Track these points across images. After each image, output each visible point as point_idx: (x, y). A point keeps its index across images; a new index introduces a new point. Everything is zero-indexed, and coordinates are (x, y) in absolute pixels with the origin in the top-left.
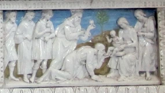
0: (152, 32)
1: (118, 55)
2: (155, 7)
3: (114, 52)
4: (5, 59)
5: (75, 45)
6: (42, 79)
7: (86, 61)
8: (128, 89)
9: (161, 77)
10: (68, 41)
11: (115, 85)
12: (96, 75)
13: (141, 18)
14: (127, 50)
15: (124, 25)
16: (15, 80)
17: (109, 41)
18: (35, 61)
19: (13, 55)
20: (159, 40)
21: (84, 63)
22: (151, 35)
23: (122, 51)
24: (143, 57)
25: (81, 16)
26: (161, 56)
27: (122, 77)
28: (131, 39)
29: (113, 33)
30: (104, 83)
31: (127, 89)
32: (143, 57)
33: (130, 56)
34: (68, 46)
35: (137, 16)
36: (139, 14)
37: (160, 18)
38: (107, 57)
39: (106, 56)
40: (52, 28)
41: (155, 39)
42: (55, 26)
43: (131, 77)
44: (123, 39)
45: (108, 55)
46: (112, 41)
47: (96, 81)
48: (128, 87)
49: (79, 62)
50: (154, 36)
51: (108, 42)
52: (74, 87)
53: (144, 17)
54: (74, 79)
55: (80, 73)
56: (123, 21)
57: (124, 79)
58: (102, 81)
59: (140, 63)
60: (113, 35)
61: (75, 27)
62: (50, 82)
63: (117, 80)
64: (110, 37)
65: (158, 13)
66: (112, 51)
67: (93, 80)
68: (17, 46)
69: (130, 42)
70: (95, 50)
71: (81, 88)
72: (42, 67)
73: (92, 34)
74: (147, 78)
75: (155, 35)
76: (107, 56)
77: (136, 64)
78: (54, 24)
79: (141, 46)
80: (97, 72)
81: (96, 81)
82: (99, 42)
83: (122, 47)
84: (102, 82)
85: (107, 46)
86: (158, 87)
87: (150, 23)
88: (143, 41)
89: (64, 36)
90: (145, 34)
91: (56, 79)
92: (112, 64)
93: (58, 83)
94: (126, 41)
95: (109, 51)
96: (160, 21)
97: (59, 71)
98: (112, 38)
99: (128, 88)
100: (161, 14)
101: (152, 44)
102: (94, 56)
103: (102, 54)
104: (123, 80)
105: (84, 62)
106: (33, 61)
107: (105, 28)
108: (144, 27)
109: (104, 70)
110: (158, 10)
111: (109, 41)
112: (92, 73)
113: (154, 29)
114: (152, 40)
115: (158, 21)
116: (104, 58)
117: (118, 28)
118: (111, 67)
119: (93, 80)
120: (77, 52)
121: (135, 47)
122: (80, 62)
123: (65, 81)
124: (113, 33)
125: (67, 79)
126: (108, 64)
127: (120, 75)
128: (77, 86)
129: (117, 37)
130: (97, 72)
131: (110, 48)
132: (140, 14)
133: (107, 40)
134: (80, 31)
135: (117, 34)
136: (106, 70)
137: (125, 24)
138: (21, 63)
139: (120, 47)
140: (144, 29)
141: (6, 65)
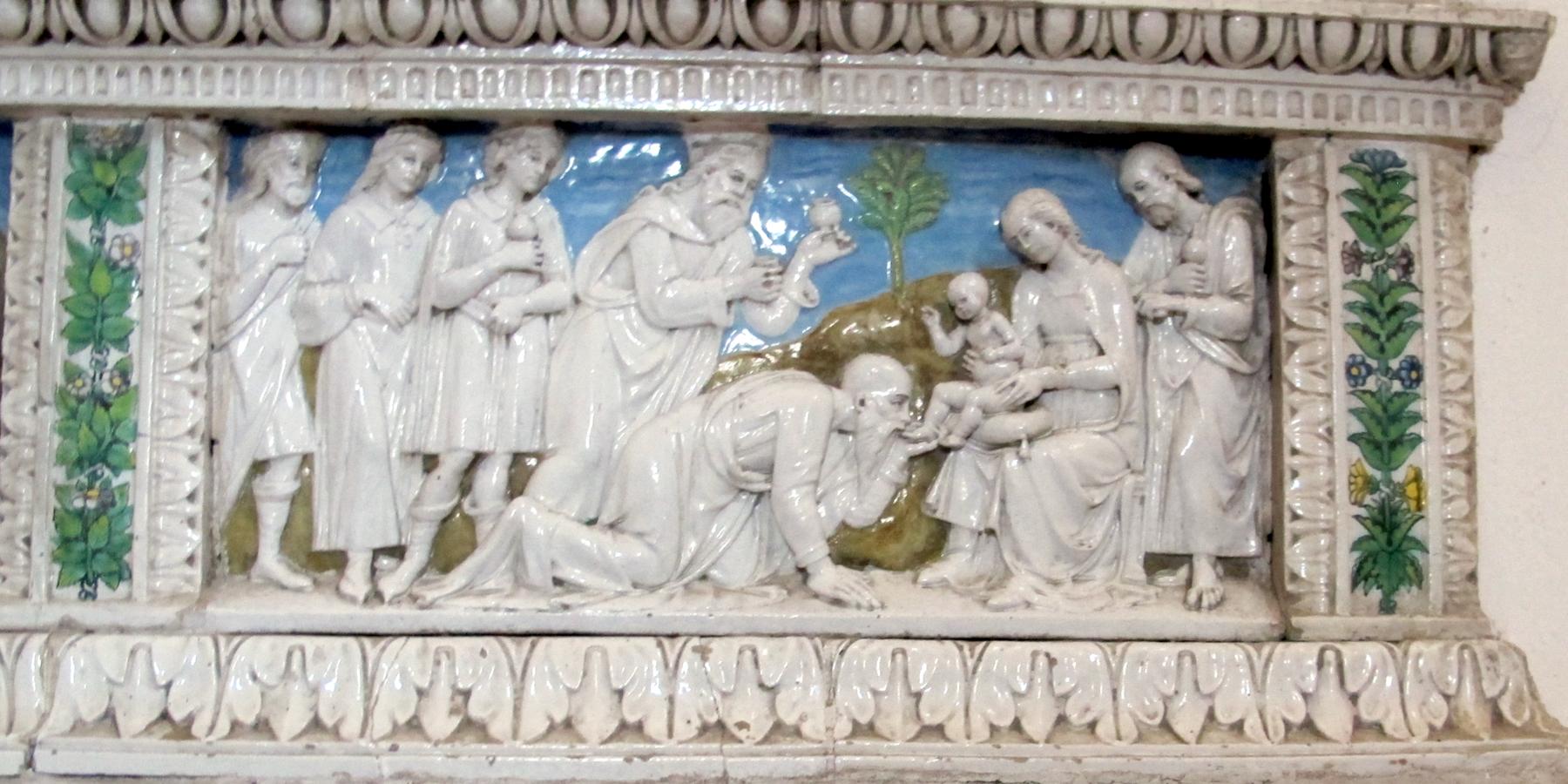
0: (1234, 295)
1: (1001, 438)
2: (1261, 122)
3: (971, 413)
4: (225, 448)
5: (704, 359)
6: (458, 578)
7: (768, 470)
8: (1052, 662)
9: (1290, 587)
10: (655, 336)
11: (965, 634)
12: (842, 568)
13: (1165, 200)
14: (1060, 405)
15: (1040, 239)
16: (284, 588)
17: (946, 343)
18: (430, 462)
19: (277, 420)
20: (1284, 346)
21: (754, 483)
22: (1237, 312)
23: (1029, 405)
24: (1171, 458)
25: (749, 166)
26: (1295, 452)
27: (1021, 585)
28: (1090, 333)
29: (970, 288)
30: (885, 614)
31: (1042, 662)
32: (1171, 458)
33: (1080, 445)
34: (657, 367)
35: (1141, 187)
36: (1149, 171)
37: (1288, 202)
38: (921, 447)
39: (916, 441)
40: (555, 245)
41: (1258, 350)
42: (578, 233)
43: (1081, 590)
44: (1042, 333)
45: (927, 434)
46: (967, 345)
47: (837, 602)
48: (1054, 648)
49: (725, 473)
50: (1255, 326)
51: (935, 354)
52: (673, 636)
53: (1184, 197)
54: (686, 586)
55: (733, 546)
56: (1035, 212)
57: (1036, 598)
58: (876, 603)
59: (1154, 495)
60: (964, 300)
61: (712, 244)
62: (511, 603)
63: (984, 602)
64: (955, 317)
65: (1282, 169)
66: (955, 409)
67: (816, 596)
68: (311, 357)
69: (1087, 350)
70: (842, 399)
71: (715, 644)
72: (474, 505)
73: (827, 291)
74: (1192, 597)
75: (1256, 315)
76: (926, 439)
77: (1124, 501)
78: (569, 223)
79: (1164, 386)
80: (853, 551)
81: (837, 602)
82: (873, 346)
83: (1030, 381)
84: (871, 608)
85: (926, 379)
86: (1259, 651)
87: (1226, 237)
88: (1173, 355)
89: (623, 296)
90: (1191, 305)
91: (558, 582)
92: (959, 493)
93: (566, 607)
94: (1061, 349)
95: (937, 408)
96: (1289, 222)
97: (589, 539)
98: (966, 322)
99: (1047, 655)
100: (1301, 180)
101: (1232, 372)
102: (832, 446)
103: (885, 428)
104: (1028, 605)
105: (761, 477)
106: (419, 461)
107: (924, 257)
108: (1183, 261)
109: (902, 539)
110: (1281, 148)
111: (946, 343)
112: (815, 552)
113: (1247, 275)
114: (1239, 345)
115: (1280, 225)
116: (900, 454)
117: (1013, 264)
118: (951, 518)
119: (816, 596)
120: (708, 404)
121: (1117, 388)
122: (730, 473)
123: (622, 594)
124: (970, 288)
125: (635, 585)
126: (931, 498)
127: (1007, 568)
128: (692, 635)
129: (998, 318)
130: (853, 551)
131: (947, 390)
132: (1156, 169)
133: (926, 342)
134: (739, 272)
135: (1003, 302)
136: (917, 539)
137: (1050, 225)
138: (331, 471)
139: (1008, 381)
140: (1187, 274)
141: (233, 489)
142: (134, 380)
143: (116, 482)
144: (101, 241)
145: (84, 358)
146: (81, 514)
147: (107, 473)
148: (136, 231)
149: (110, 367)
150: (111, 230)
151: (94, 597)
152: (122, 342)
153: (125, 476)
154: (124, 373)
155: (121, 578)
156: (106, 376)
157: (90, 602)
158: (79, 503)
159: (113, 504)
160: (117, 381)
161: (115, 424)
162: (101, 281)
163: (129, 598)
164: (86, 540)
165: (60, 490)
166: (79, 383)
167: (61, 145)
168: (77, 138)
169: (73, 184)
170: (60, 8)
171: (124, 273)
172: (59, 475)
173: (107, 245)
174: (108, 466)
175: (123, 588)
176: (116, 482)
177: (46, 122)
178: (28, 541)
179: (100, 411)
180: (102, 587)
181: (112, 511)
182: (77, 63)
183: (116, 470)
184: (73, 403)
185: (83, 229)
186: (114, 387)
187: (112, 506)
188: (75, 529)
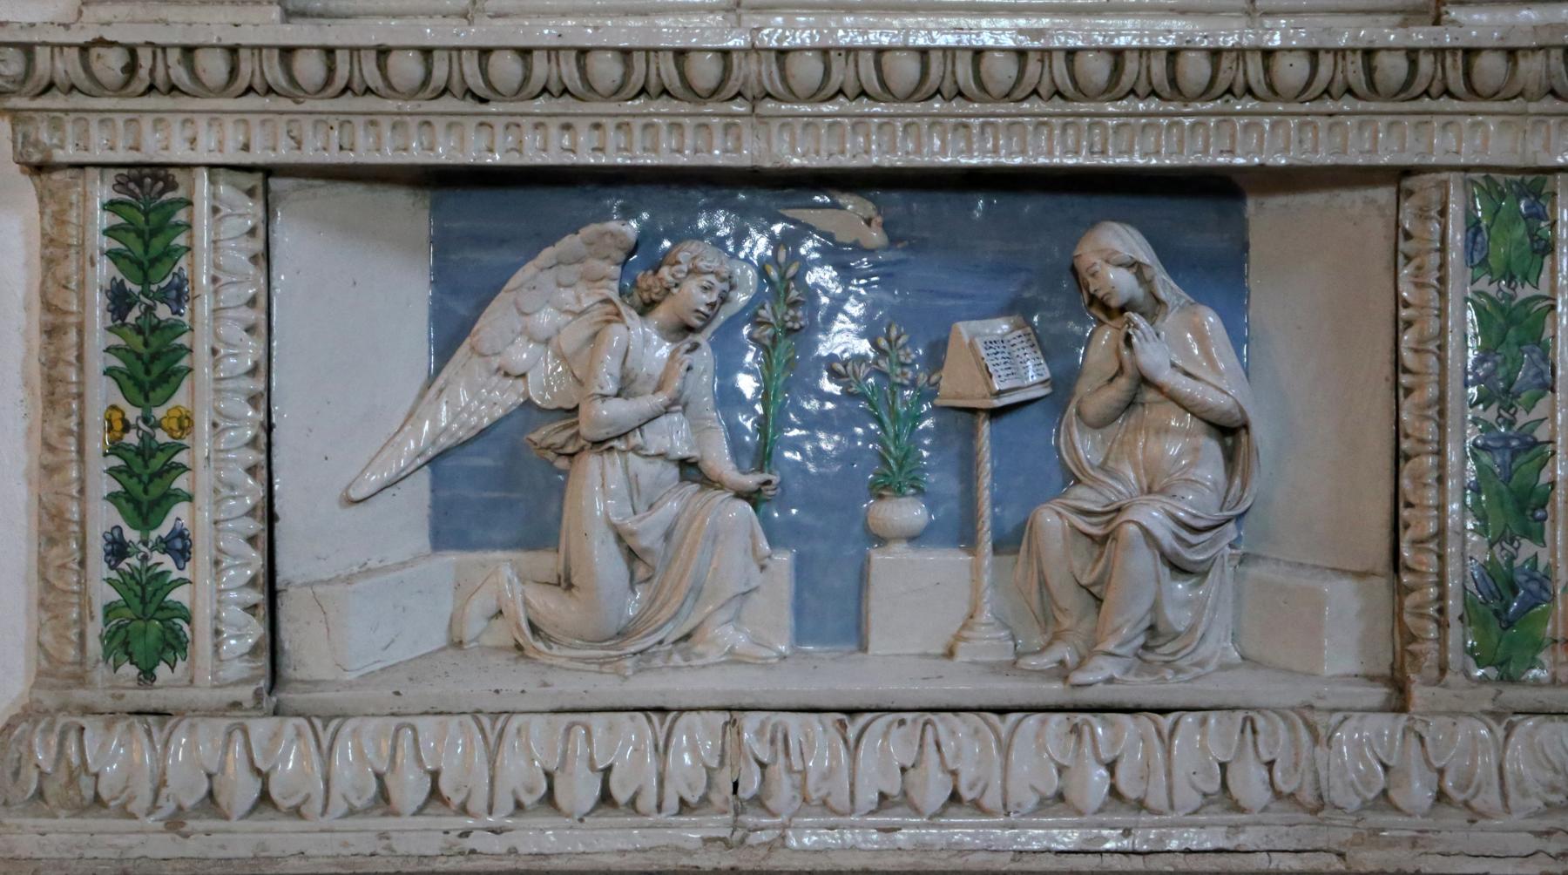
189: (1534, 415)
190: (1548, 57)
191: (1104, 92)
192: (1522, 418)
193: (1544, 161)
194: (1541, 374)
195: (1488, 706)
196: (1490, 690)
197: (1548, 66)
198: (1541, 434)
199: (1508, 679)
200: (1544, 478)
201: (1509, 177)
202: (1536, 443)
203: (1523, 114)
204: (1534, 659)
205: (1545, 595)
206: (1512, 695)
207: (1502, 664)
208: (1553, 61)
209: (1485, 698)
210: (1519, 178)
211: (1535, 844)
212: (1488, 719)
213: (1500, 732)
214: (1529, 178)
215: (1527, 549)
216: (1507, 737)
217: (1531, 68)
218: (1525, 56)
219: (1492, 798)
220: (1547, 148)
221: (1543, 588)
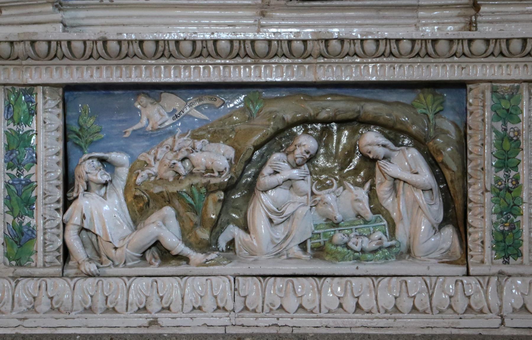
142: (520, 183)
143: (515, 221)
144: (506, 130)
145: (501, 174)
146: (502, 232)
147: (512, 217)
148: (519, 126)
149: (511, 177)
150: (509, 125)
151: (509, 263)
152: (515, 168)
153: (519, 218)
154: (517, 179)
155: (518, 256)
156: (510, 181)
157: (507, 265)
158: (502, 228)
159: (515, 228)
160: (514, 183)
161: (514, 198)
162: (507, 145)
163: (522, 264)
164: (505, 242)
165: (496, 224)
166: (500, 183)
167: (488, 94)
168: (494, 91)
169: (494, 109)
170: (500, 45)
171: (516, 143)
172: (495, 218)
173: (508, 132)
174: (512, 214)
175: (519, 260)
176: (515, 221)
177: (482, 85)
178: (483, 242)
179: (508, 194)
180: (511, 260)
181: (514, 231)
182: (498, 64)
183: (515, 216)
184: (498, 191)
185: (499, 126)
186: (513, 185)
187: (514, 228)
188: (500, 238)
189: (31, 172)
190: (25, 45)
191: (190, 56)
192: (26, 173)
193: (30, 81)
194: (32, 157)
195: (11, 275)
196: (12, 269)
197: (25, 48)
198: (33, 179)
199: (19, 265)
200: (33, 195)
201: (21, 88)
202: (31, 182)
203: (21, 65)
204: (29, 258)
205: (34, 236)
206: (20, 271)
207: (17, 260)
208: (27, 46)
209: (10, 272)
210: (24, 88)
211: (19, 322)
212: (10, 279)
213: (13, 284)
214: (28, 88)
215: (27, 220)
216: (16, 286)
217: (19, 48)
218: (16, 44)
219: (9, 307)
220: (31, 77)
221: (33, 233)
